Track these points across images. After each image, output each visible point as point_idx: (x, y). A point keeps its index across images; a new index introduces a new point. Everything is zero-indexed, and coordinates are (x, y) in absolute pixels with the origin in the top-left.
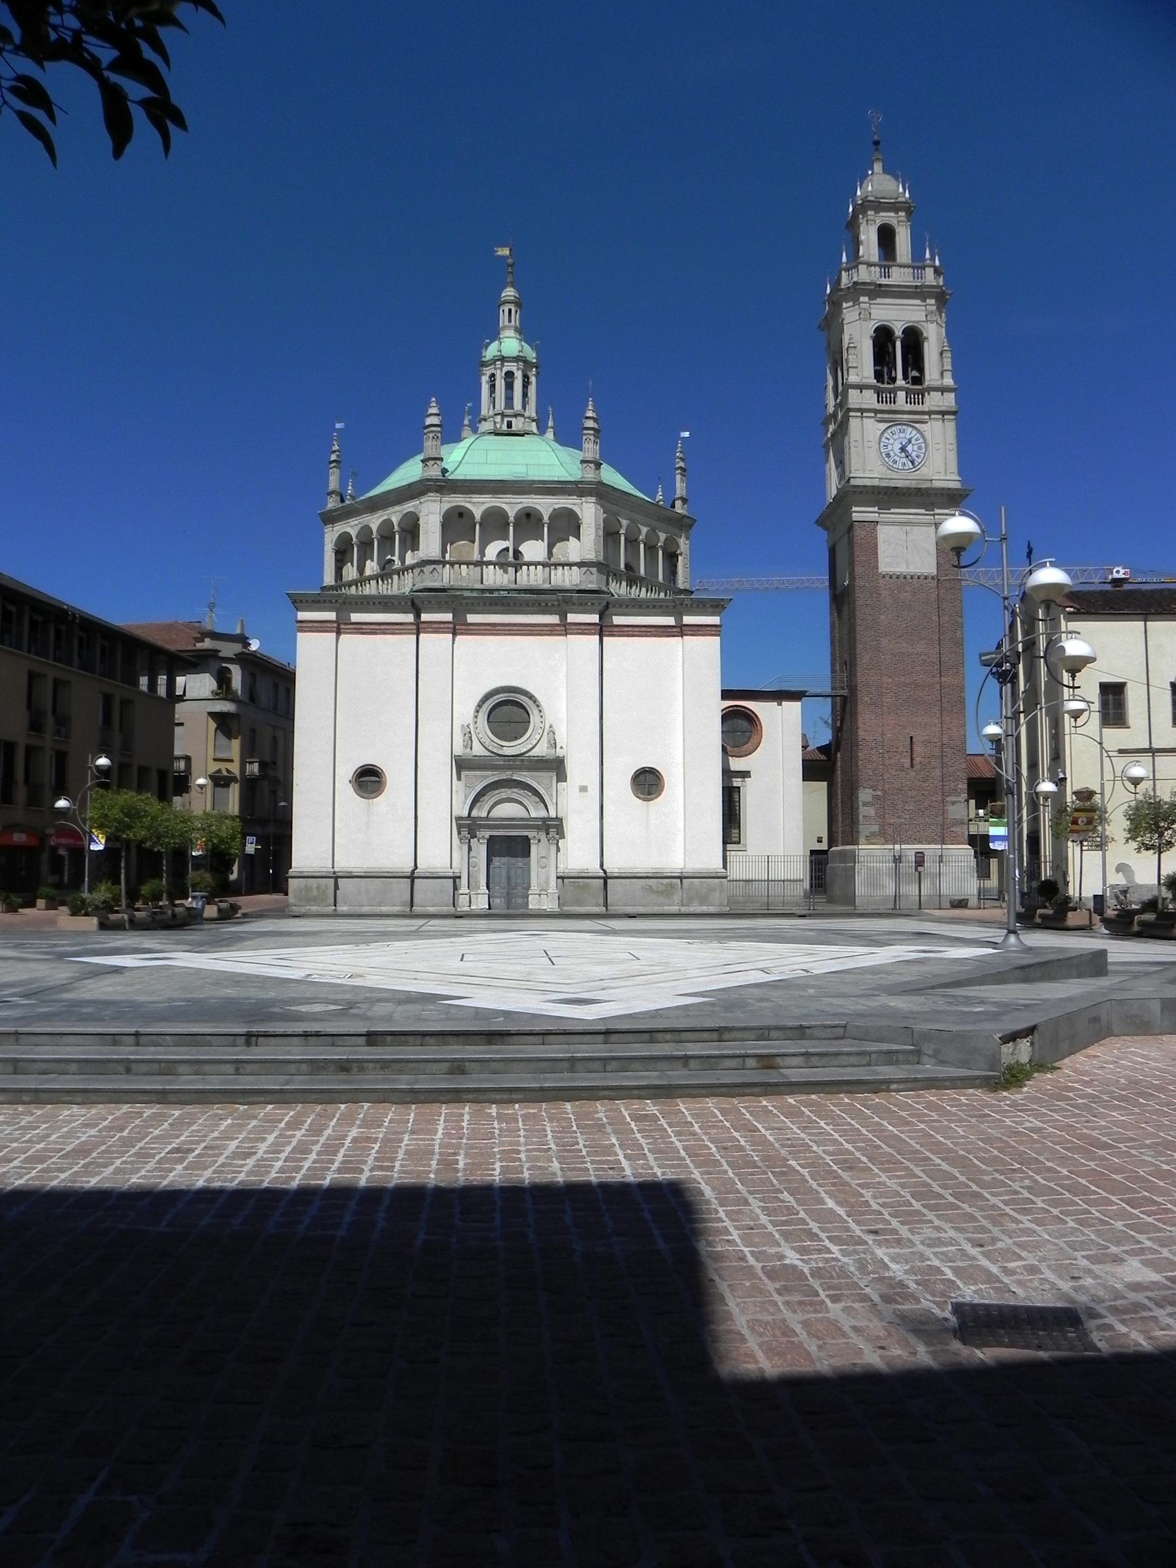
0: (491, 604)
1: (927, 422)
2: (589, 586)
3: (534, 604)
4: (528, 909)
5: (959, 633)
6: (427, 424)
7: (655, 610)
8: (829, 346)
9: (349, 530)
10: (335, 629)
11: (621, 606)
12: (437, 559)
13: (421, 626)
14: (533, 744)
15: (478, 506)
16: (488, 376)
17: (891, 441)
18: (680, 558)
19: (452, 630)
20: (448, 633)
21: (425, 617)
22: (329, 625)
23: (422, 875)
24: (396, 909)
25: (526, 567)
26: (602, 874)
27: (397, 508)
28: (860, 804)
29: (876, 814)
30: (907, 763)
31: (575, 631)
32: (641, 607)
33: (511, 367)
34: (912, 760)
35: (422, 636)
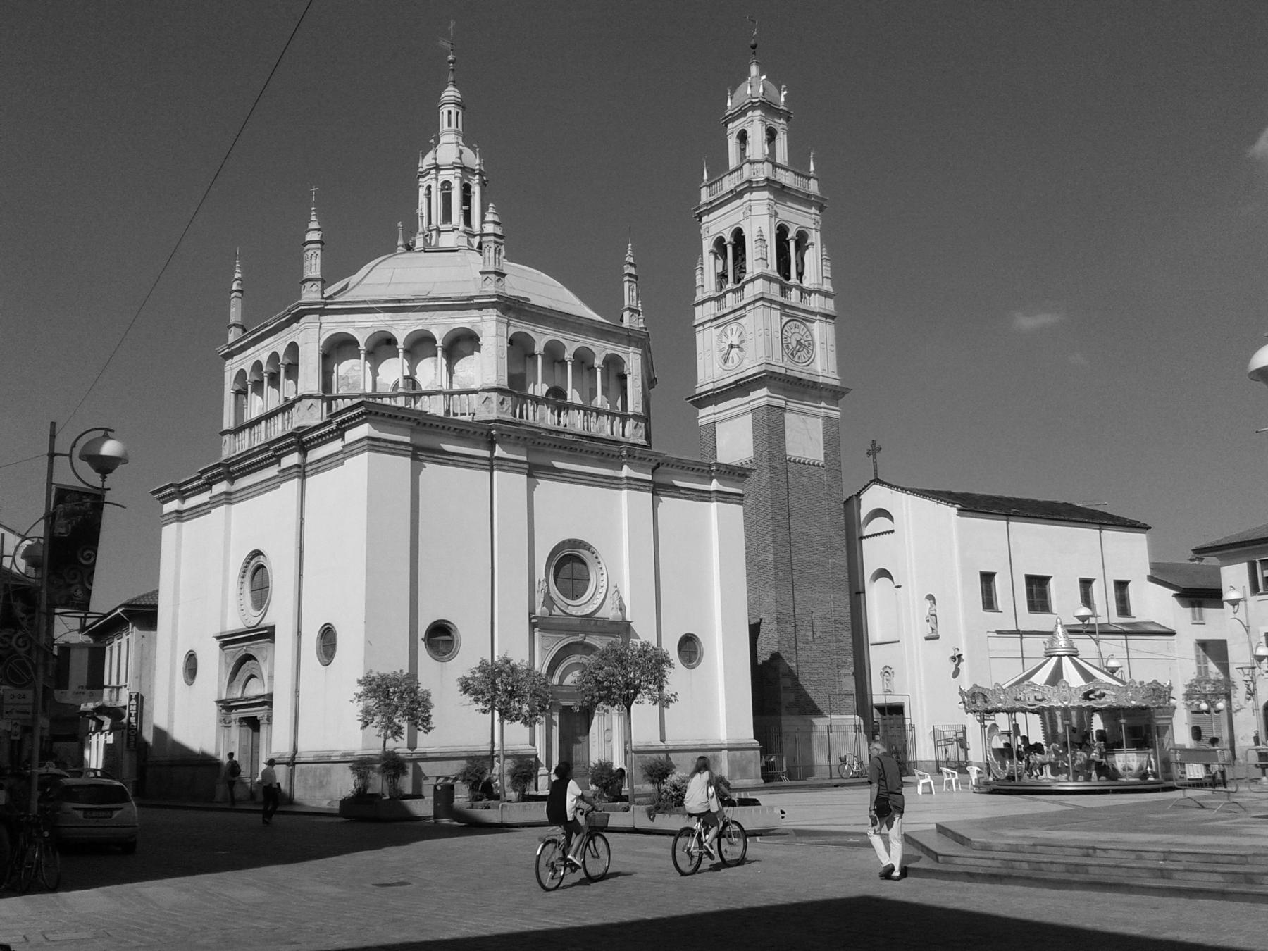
1: (814, 322)
2: (640, 440)
3: (597, 453)
7: (692, 473)
10: (410, 453)
12: (507, 387)
15: (542, 337)
19: (526, 471)
22: (402, 447)
28: (780, 675)
30: (810, 639)
31: (633, 487)
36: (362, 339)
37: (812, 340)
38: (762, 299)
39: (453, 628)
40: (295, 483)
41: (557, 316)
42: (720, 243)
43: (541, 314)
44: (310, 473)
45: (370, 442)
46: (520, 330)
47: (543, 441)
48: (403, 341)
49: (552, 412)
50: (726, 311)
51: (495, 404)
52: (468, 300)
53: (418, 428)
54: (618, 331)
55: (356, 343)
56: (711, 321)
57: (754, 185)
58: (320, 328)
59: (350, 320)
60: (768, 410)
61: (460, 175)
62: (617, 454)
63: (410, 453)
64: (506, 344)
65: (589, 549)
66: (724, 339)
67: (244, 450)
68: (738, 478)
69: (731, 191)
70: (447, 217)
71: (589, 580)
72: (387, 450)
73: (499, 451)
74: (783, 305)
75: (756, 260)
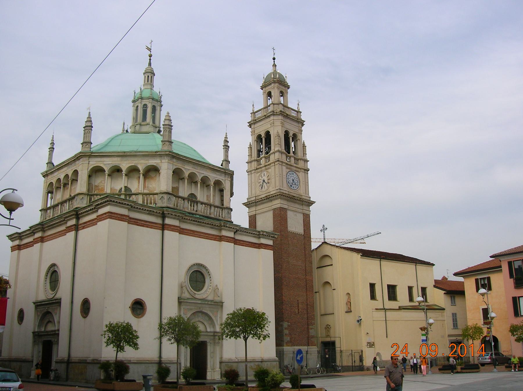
1: (300, 172)
3: (210, 224)
4: (207, 380)
5: (311, 258)
7: (251, 235)
8: (254, 132)
9: (102, 165)
12: (171, 192)
14: (206, 293)
17: (290, 177)
20: (177, 232)
22: (125, 217)
25: (204, 205)
27: (143, 161)
29: (289, 333)
30: (297, 312)
31: (226, 240)
33: (145, 102)
34: (298, 310)
36: (106, 169)
37: (299, 180)
38: (278, 161)
39: (143, 303)
40: (73, 233)
41: (194, 162)
42: (259, 137)
43: (187, 160)
44: (81, 228)
45: (110, 214)
46: (178, 167)
47: (186, 218)
48: (125, 170)
49: (191, 206)
50: (261, 166)
51: (166, 199)
52: (156, 153)
53: (132, 209)
54: (221, 170)
55: (104, 171)
56: (255, 170)
58: (89, 163)
59: (102, 160)
60: (280, 209)
62: (219, 225)
63: (127, 220)
64: (171, 173)
66: (260, 178)
67: (50, 218)
68: (271, 238)
69: (265, 115)
70: (144, 118)
71: (204, 282)
73: (168, 221)
74: (287, 164)
75: (276, 145)
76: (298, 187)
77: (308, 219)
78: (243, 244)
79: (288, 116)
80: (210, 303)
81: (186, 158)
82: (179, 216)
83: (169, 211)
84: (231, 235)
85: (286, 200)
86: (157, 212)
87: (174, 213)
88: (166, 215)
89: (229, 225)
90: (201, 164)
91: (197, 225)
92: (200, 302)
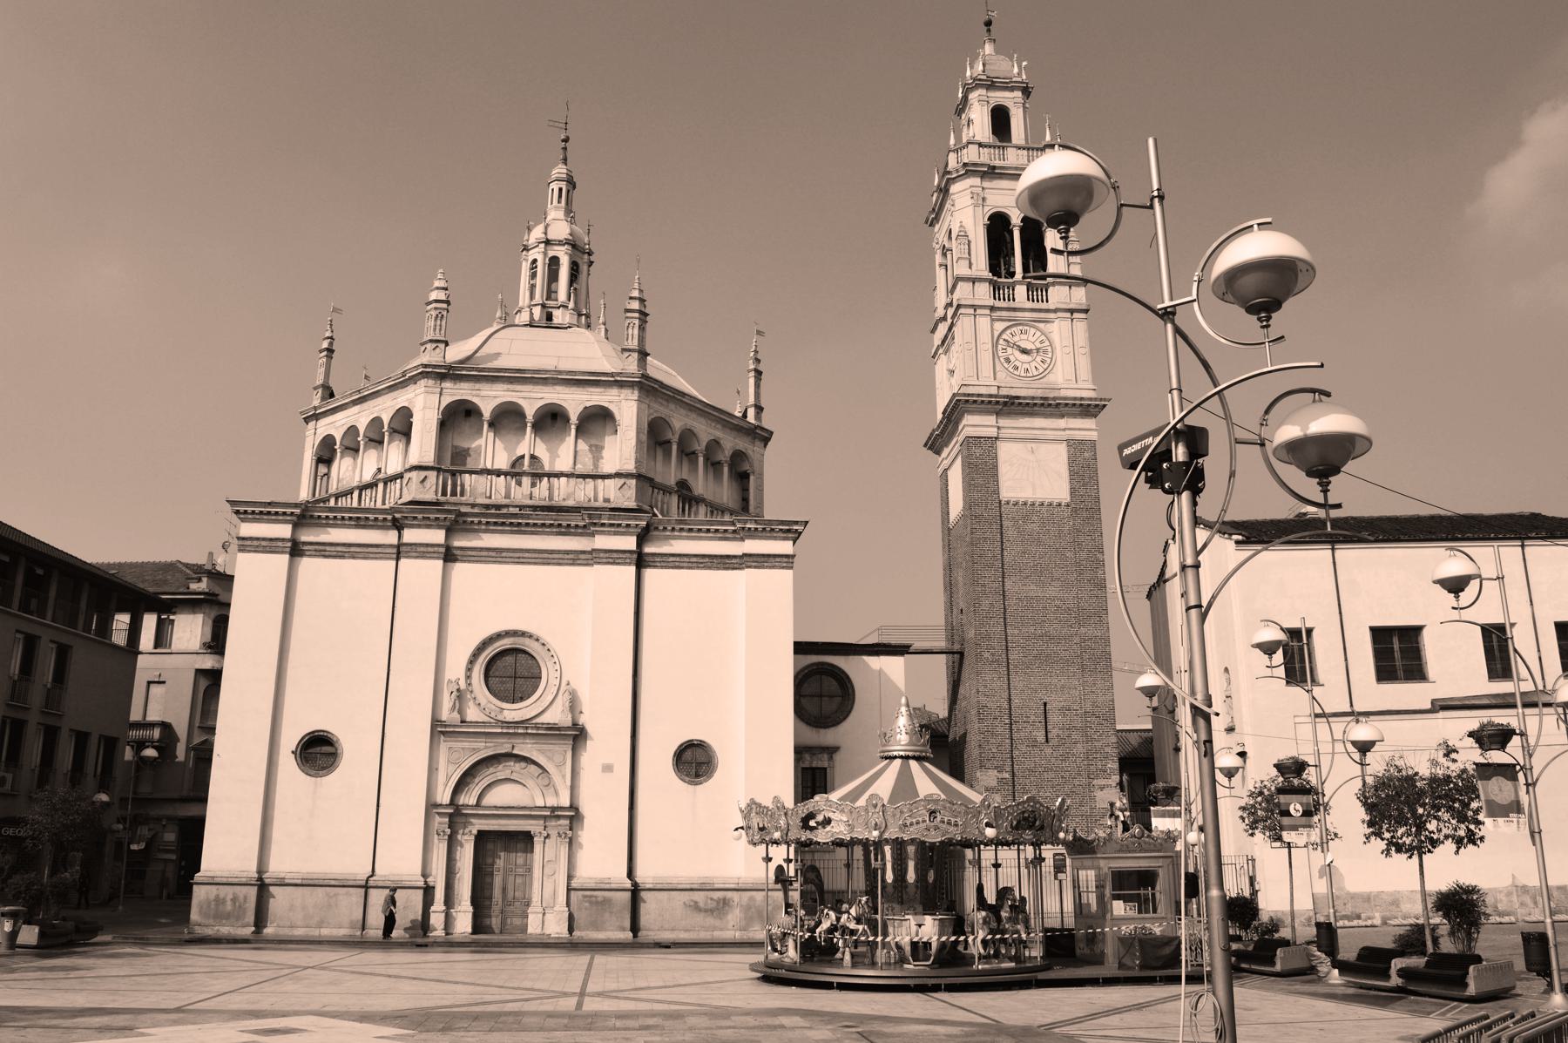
0: (496, 524)
1: (1053, 322)
3: (551, 525)
5: (1101, 572)
6: (431, 299)
8: (937, 243)
10: (288, 550)
11: (665, 529)
12: (431, 464)
13: (403, 549)
16: (529, 262)
18: (752, 478)
19: (442, 556)
20: (438, 558)
21: (411, 535)
22: (280, 544)
23: (380, 884)
24: (342, 932)
26: (628, 884)
27: (389, 403)
30: (1041, 738)
31: (604, 560)
32: (691, 530)
35: (403, 562)
37: (1051, 345)
39: (335, 739)
41: (506, 374)
52: (403, 376)
53: (304, 521)
57: (953, 176)
58: (315, 434)
61: (543, 250)
65: (537, 640)
71: (541, 678)
72: (261, 549)
76: (1045, 367)
77: (1086, 454)
78: (677, 564)
79: (996, 171)
80: (534, 732)
81: (479, 371)
82: (437, 519)
83: (405, 510)
84: (629, 543)
85: (988, 413)
86: (376, 519)
87: (420, 513)
88: (401, 521)
89: (609, 519)
90: (530, 376)
91: (512, 532)
92: (499, 730)
